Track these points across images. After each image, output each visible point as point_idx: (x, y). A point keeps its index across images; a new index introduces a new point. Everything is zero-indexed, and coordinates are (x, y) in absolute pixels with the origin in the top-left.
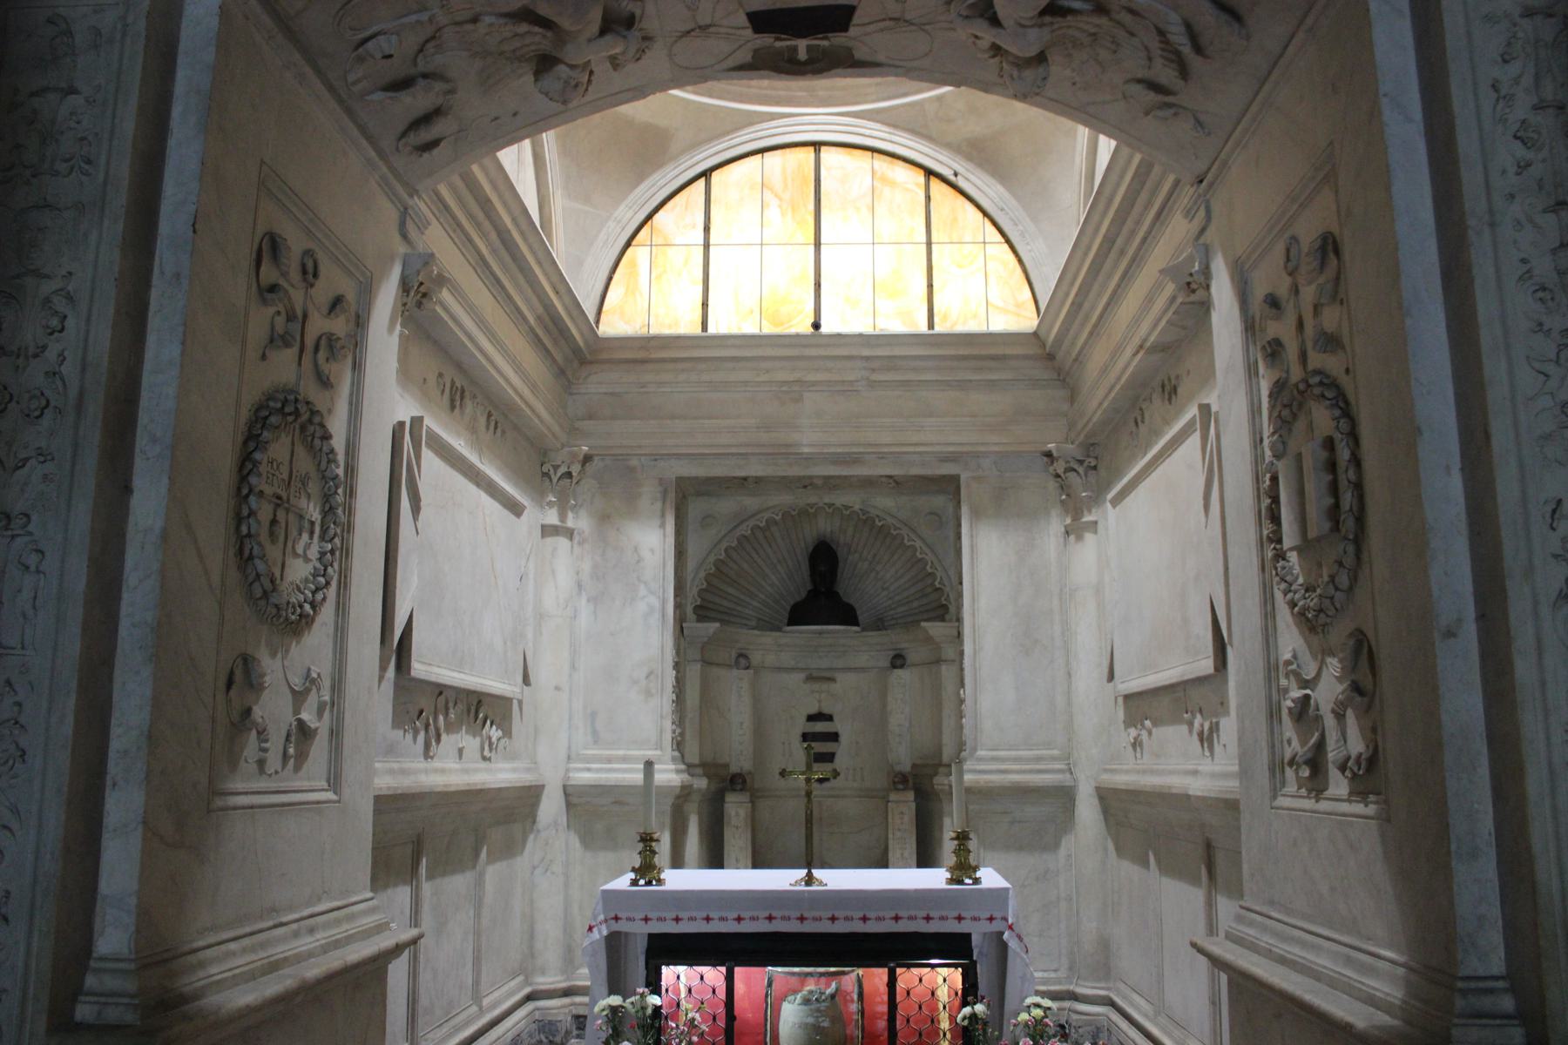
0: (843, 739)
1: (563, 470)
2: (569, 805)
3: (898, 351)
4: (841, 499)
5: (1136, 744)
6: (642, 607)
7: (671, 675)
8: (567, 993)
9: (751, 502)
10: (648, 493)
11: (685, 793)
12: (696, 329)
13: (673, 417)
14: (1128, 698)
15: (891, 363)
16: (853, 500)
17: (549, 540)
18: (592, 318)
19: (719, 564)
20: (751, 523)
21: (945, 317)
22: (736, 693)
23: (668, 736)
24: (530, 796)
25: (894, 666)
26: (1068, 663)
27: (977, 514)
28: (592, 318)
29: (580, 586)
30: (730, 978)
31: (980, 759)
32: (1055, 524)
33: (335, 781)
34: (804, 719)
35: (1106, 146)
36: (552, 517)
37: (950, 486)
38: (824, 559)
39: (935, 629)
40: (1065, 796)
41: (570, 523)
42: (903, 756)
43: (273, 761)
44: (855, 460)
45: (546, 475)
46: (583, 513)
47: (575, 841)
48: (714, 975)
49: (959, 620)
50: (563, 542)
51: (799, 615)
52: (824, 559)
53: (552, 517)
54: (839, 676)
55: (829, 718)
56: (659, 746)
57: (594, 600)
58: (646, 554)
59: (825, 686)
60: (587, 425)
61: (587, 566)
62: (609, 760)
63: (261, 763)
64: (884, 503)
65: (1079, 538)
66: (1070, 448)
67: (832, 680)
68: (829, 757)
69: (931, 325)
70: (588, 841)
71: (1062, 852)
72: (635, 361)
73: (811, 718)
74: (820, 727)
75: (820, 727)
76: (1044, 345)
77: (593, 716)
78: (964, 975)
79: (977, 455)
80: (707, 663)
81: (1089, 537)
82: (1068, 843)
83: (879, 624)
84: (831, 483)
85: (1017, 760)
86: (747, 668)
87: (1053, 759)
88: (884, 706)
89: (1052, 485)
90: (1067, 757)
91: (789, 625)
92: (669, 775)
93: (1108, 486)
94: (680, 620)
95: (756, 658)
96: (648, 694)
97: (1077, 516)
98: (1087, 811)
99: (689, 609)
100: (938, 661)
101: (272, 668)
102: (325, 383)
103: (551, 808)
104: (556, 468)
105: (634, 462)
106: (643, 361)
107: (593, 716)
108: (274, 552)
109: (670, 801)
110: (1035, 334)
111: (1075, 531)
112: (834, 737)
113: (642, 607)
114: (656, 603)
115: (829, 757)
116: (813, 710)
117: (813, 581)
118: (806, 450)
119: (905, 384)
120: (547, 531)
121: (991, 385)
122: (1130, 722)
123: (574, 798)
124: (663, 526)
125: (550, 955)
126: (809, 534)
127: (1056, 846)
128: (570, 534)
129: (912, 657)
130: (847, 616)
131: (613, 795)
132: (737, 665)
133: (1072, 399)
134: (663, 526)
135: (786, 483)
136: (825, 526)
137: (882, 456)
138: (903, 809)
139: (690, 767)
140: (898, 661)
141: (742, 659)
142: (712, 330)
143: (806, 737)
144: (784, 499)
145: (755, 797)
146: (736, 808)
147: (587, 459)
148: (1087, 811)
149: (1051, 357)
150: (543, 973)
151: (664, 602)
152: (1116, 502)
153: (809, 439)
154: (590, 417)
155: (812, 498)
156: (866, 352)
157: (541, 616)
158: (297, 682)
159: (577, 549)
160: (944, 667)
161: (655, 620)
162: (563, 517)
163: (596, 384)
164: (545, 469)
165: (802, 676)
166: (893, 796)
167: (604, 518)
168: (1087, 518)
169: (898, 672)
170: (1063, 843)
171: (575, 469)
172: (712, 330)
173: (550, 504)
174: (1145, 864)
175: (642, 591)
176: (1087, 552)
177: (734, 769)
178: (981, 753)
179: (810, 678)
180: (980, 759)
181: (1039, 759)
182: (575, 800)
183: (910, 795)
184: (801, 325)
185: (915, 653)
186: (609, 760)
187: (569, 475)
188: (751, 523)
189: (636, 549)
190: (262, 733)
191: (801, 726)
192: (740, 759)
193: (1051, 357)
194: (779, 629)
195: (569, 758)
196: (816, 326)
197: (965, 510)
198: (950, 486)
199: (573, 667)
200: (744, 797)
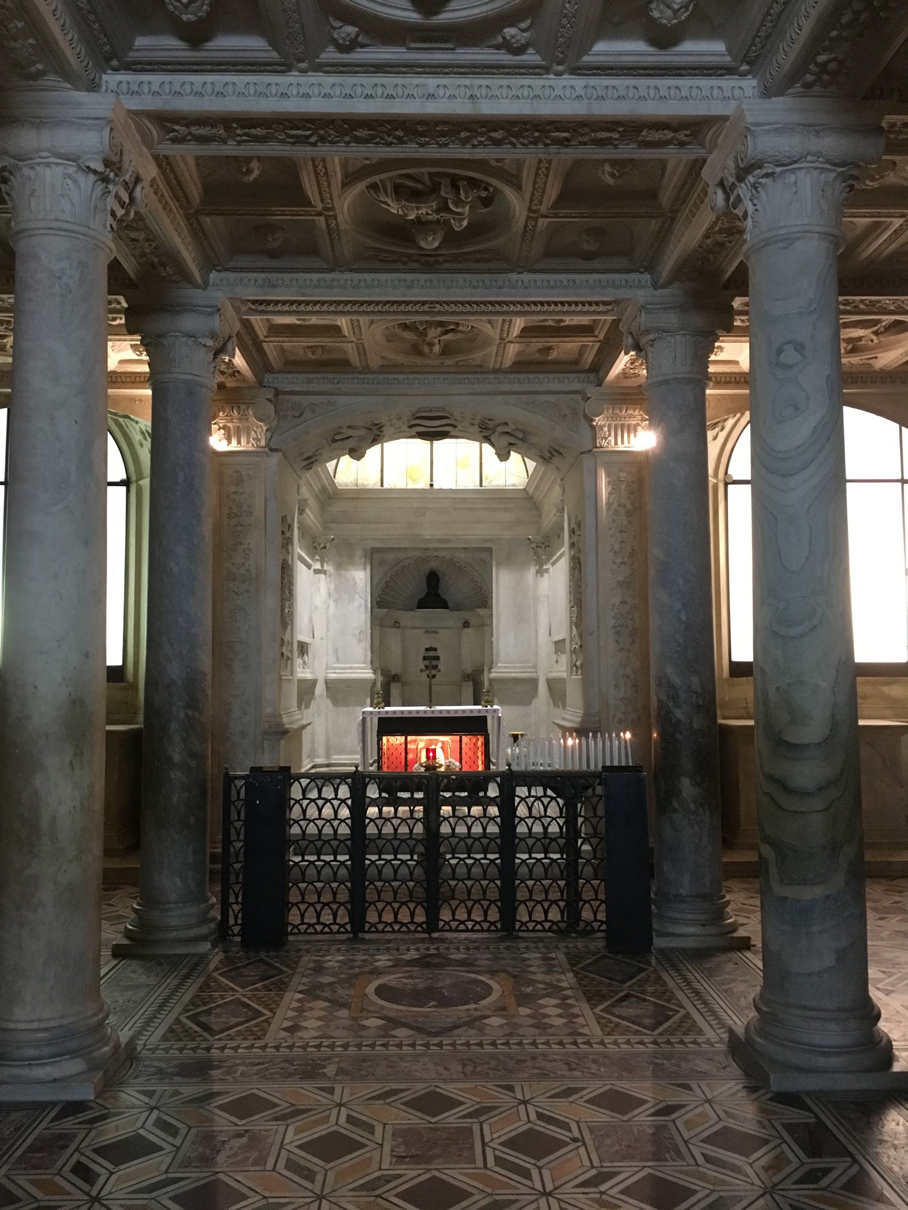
0: (441, 659)
1: (322, 545)
2: (327, 688)
3: (467, 496)
4: (440, 554)
5: (557, 662)
6: (356, 603)
7: (369, 631)
8: (328, 765)
9: (401, 556)
10: (359, 553)
11: (374, 683)
12: (378, 487)
13: (370, 523)
14: (556, 643)
15: (464, 500)
16: (447, 555)
17: (318, 576)
18: (332, 474)
19: (386, 583)
20: (401, 564)
21: (487, 478)
22: (394, 639)
23: (369, 658)
24: (314, 682)
25: (464, 627)
26: (536, 627)
27: (499, 564)
28: (332, 474)
29: (330, 595)
30: (406, 739)
31: (500, 667)
32: (533, 570)
33: (292, 675)
34: (423, 650)
35: (531, 465)
36: (318, 566)
37: (489, 550)
38: (433, 579)
39: (481, 611)
40: (534, 682)
41: (326, 568)
42: (468, 667)
44: (448, 541)
45: (315, 548)
46: (330, 563)
47: (329, 702)
48: (400, 740)
49: (492, 608)
50: (322, 576)
51: (422, 605)
52: (433, 579)
53: (318, 566)
54: (440, 631)
55: (435, 650)
56: (365, 662)
57: (336, 601)
58: (357, 580)
59: (433, 635)
60: (333, 525)
61: (332, 586)
62: (344, 668)
64: (460, 555)
65: (542, 576)
66: (539, 538)
67: (437, 632)
68: (435, 667)
69: (481, 485)
70: (335, 703)
71: (533, 705)
72: (353, 498)
73: (427, 650)
74: (431, 654)
75: (431, 654)
76: (528, 493)
77: (337, 650)
78: (485, 739)
79: (500, 539)
80: (382, 626)
81: (546, 575)
82: (535, 702)
83: (458, 608)
84: (436, 549)
85: (515, 667)
86: (398, 628)
87: (530, 667)
88: (460, 644)
89: (531, 552)
90: (535, 666)
91: (419, 607)
92: (367, 674)
93: (552, 556)
94: (372, 608)
95: (402, 623)
96: (360, 641)
97: (541, 567)
98: (543, 688)
99: (374, 602)
100: (483, 625)
102: (288, 553)
103: (320, 689)
104: (319, 544)
105: (352, 541)
106: (358, 498)
107: (337, 650)
109: (370, 685)
110: (524, 489)
111: (540, 572)
112: (438, 658)
113: (356, 603)
114: (363, 602)
115: (435, 667)
116: (428, 647)
117: (428, 588)
118: (427, 537)
119: (469, 509)
120: (317, 572)
121: (506, 510)
122: (556, 653)
123: (330, 685)
124: (365, 569)
125: (321, 750)
126: (427, 568)
127: (530, 703)
128: (325, 572)
129: (472, 622)
130: (444, 605)
131: (348, 683)
132: (395, 627)
133: (540, 516)
134: (365, 569)
135: (419, 549)
136: (434, 565)
137: (459, 540)
138: (468, 689)
139: (375, 673)
140: (466, 624)
141: (396, 624)
142: (386, 486)
143: (425, 658)
144: (417, 554)
145: (404, 685)
146: (395, 690)
147: (333, 539)
148: (543, 688)
149: (531, 498)
150: (318, 757)
151: (366, 601)
152: (553, 564)
153: (428, 532)
154: (333, 522)
155: (428, 553)
156: (453, 496)
157: (316, 608)
159: (328, 579)
160: (485, 628)
161: (362, 609)
162: (322, 566)
163: (336, 508)
164: (315, 544)
165: (423, 631)
166: (464, 684)
167: (339, 566)
168: (545, 567)
169: (466, 629)
170: (534, 702)
171: (328, 546)
172: (386, 486)
173: (317, 560)
174: (559, 707)
175: (357, 596)
176: (545, 583)
177: (393, 673)
178: (499, 665)
179: (427, 632)
180: (500, 667)
181: (523, 667)
182: (330, 685)
183: (471, 683)
184: (423, 484)
185: (472, 622)
186: (344, 668)
187: (325, 547)
188: (401, 564)
189: (354, 578)
191: (422, 653)
192: (396, 670)
193: (531, 498)
194: (412, 610)
195: (327, 668)
196: (432, 485)
197: (494, 562)
198: (489, 550)
199: (328, 630)
200: (399, 685)
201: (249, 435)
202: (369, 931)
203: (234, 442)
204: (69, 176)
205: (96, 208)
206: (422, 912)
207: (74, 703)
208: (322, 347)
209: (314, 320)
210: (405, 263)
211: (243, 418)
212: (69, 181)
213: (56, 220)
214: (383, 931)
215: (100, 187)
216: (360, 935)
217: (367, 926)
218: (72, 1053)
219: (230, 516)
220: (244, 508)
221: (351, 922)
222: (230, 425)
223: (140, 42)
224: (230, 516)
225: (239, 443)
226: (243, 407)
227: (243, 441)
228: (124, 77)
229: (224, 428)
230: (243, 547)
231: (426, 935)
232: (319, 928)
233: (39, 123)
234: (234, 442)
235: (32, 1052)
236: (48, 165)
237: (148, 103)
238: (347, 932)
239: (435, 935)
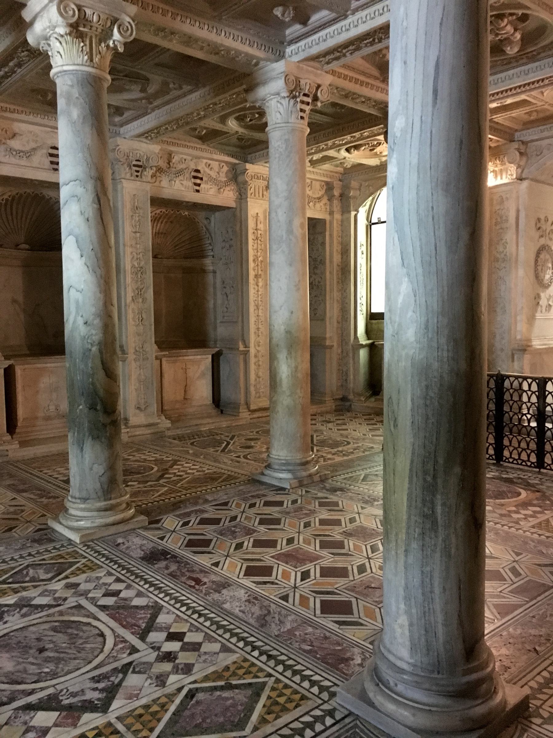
43: (544, 310)
63: (541, 312)
101: (542, 295)
108: (542, 275)
158: (548, 296)
190: (541, 306)
201: (507, 172)
202: (505, 461)
203: (499, 177)
204: (278, 102)
205: (291, 112)
206: (535, 456)
207: (287, 332)
208: (536, 111)
209: (509, 101)
210: (517, 61)
211: (503, 164)
212: (279, 105)
213: (276, 124)
214: (512, 463)
215: (292, 101)
216: (501, 463)
217: (504, 458)
218: (289, 471)
219: (496, 224)
220: (504, 218)
221: (495, 454)
222: (496, 169)
223: (288, 32)
224: (496, 224)
225: (501, 178)
226: (501, 157)
227: (504, 176)
228: (293, 47)
229: (494, 171)
230: (503, 241)
231: (538, 470)
232: (511, 460)
233: (264, 83)
234: (499, 177)
235: (277, 467)
236: (271, 99)
237: (302, 56)
238: (493, 459)
239: (542, 470)
